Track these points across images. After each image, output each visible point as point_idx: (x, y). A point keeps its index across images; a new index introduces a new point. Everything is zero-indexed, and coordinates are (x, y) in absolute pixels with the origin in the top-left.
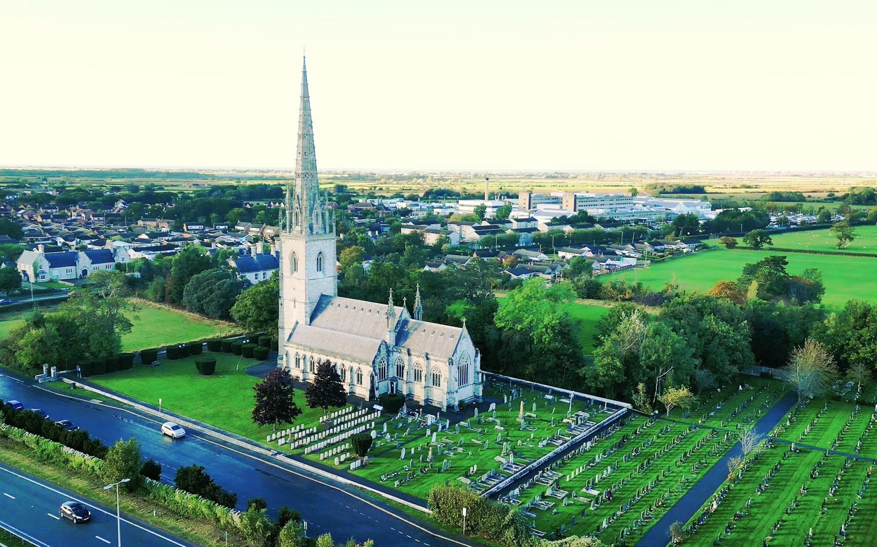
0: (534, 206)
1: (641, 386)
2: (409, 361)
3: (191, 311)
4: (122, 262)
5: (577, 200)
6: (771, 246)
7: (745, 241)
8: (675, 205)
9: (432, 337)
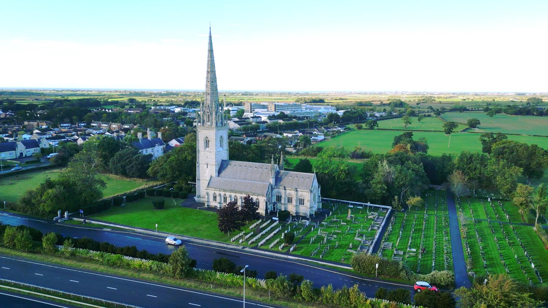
0: (253, 109)
1: (396, 197)
2: (285, 193)
3: (117, 174)
4: (44, 147)
5: (276, 107)
6: (378, 128)
7: (366, 125)
8: (320, 108)
9: (296, 179)
